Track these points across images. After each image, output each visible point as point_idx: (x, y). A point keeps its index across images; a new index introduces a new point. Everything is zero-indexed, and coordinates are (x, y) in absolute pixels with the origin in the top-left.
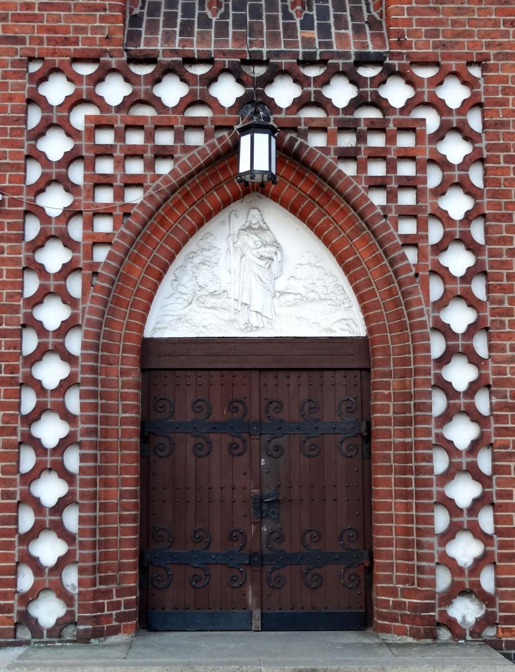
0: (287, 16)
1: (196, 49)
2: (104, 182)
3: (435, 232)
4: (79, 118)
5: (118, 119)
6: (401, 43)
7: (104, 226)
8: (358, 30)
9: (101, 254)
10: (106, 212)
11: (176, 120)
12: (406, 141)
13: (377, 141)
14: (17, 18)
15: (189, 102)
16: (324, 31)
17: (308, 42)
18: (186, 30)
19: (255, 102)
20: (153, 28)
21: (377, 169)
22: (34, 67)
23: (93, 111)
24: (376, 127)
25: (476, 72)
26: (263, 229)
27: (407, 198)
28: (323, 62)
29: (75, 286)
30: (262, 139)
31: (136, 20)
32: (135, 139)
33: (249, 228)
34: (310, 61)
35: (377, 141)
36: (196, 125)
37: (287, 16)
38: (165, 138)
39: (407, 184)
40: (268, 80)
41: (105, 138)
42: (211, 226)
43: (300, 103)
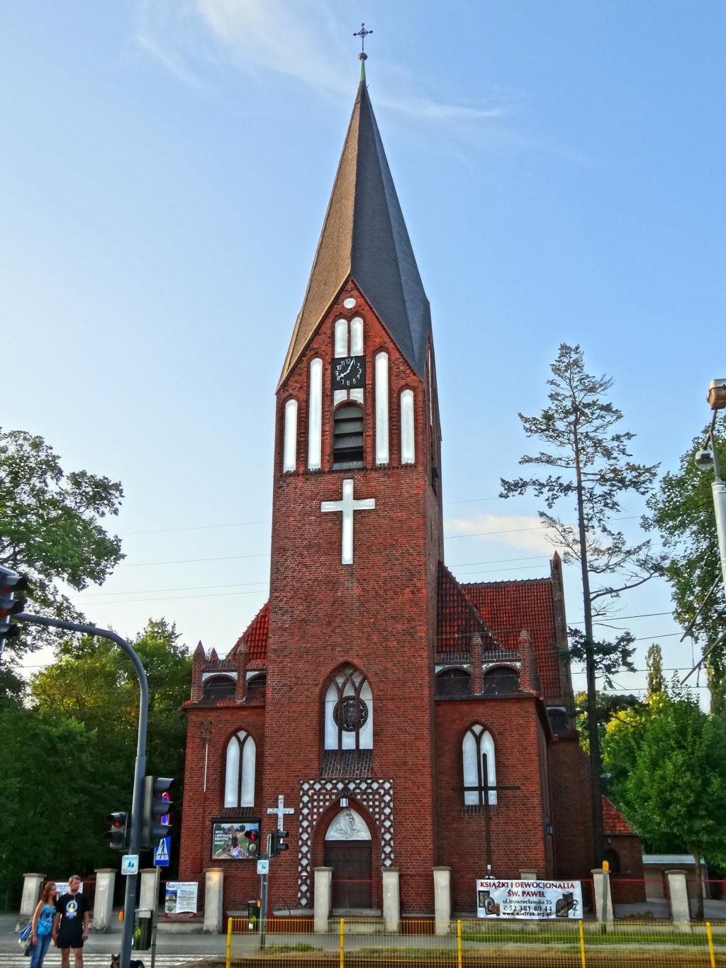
0: (354, 767)
1: (334, 777)
2: (315, 807)
3: (383, 817)
4: (310, 792)
5: (318, 793)
6: (376, 775)
7: (315, 817)
8: (368, 770)
9: (314, 823)
10: (315, 813)
11: (329, 792)
12: (377, 797)
13: (371, 797)
14: (298, 771)
15: (332, 789)
16: (361, 772)
17: (357, 774)
18: (332, 772)
19: (346, 788)
20: (325, 772)
21: (371, 803)
22: (301, 782)
23: (313, 791)
24: (370, 793)
25: (391, 781)
26: (351, 815)
27: (377, 810)
28: (359, 779)
29: (309, 830)
30: (344, 800)
31: (322, 769)
32: (321, 797)
33: (347, 815)
34: (357, 779)
35: (371, 797)
36: (334, 794)
37: (354, 767)
38: (327, 797)
39: (377, 806)
40: (349, 783)
41: (315, 797)
42: (340, 814)
43: (355, 789)
